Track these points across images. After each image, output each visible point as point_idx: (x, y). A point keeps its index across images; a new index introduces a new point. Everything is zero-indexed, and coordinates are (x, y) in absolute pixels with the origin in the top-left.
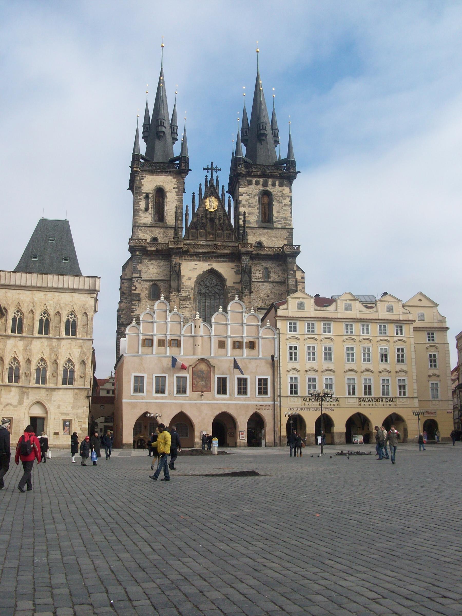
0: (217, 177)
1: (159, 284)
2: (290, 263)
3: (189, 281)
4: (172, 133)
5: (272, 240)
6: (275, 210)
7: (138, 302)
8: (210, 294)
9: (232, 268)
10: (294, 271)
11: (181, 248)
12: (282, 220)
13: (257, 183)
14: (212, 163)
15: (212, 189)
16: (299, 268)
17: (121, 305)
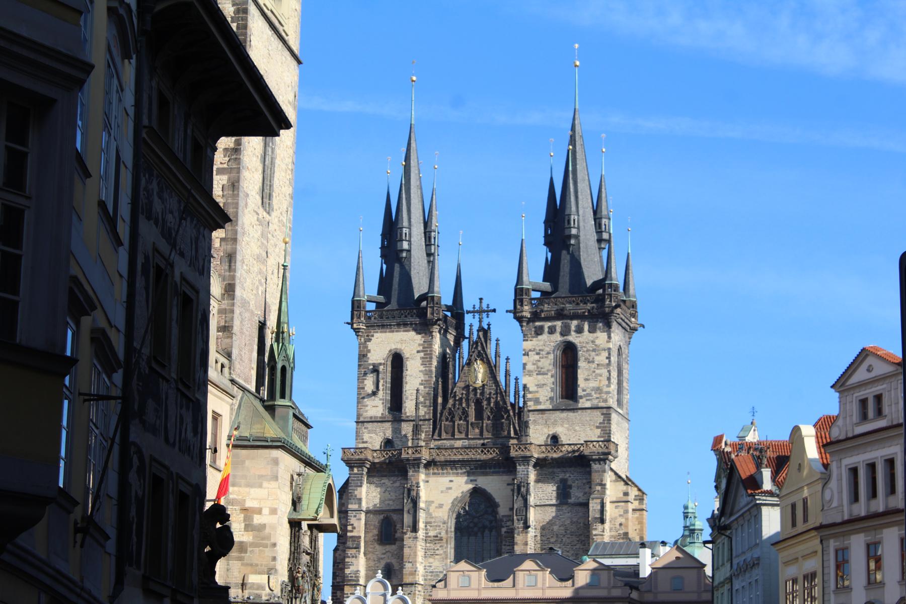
0: (489, 325)
1: (395, 517)
2: (596, 471)
3: (441, 510)
4: (426, 245)
5: (575, 430)
6: (581, 375)
7: (355, 550)
8: (476, 529)
9: (508, 484)
10: (603, 486)
11: (420, 459)
12: (593, 393)
13: (552, 331)
14: (481, 299)
15: (479, 348)
16: (620, 477)
17: (337, 555)
